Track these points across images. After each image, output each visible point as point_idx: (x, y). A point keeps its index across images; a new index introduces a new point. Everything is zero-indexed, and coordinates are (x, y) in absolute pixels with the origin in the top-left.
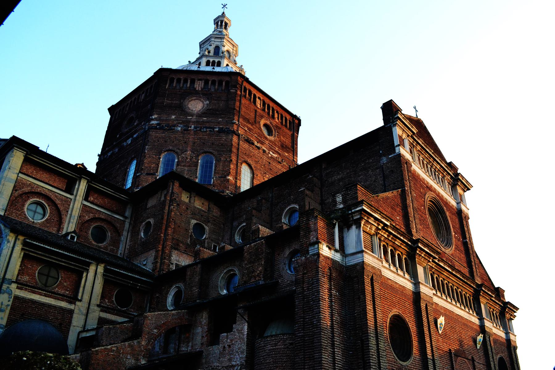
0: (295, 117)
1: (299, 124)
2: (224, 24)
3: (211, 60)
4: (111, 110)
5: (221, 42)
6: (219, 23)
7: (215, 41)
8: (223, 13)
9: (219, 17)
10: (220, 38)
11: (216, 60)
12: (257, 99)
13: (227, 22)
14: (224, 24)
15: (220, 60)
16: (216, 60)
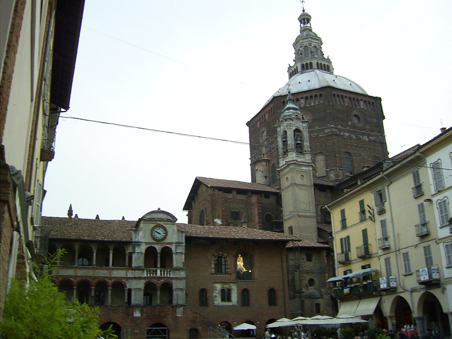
3: (304, 63)
4: (248, 124)
5: (308, 41)
7: (303, 42)
9: (301, 16)
11: (308, 62)
13: (309, 18)
14: (306, 21)
15: (311, 61)
16: (308, 62)
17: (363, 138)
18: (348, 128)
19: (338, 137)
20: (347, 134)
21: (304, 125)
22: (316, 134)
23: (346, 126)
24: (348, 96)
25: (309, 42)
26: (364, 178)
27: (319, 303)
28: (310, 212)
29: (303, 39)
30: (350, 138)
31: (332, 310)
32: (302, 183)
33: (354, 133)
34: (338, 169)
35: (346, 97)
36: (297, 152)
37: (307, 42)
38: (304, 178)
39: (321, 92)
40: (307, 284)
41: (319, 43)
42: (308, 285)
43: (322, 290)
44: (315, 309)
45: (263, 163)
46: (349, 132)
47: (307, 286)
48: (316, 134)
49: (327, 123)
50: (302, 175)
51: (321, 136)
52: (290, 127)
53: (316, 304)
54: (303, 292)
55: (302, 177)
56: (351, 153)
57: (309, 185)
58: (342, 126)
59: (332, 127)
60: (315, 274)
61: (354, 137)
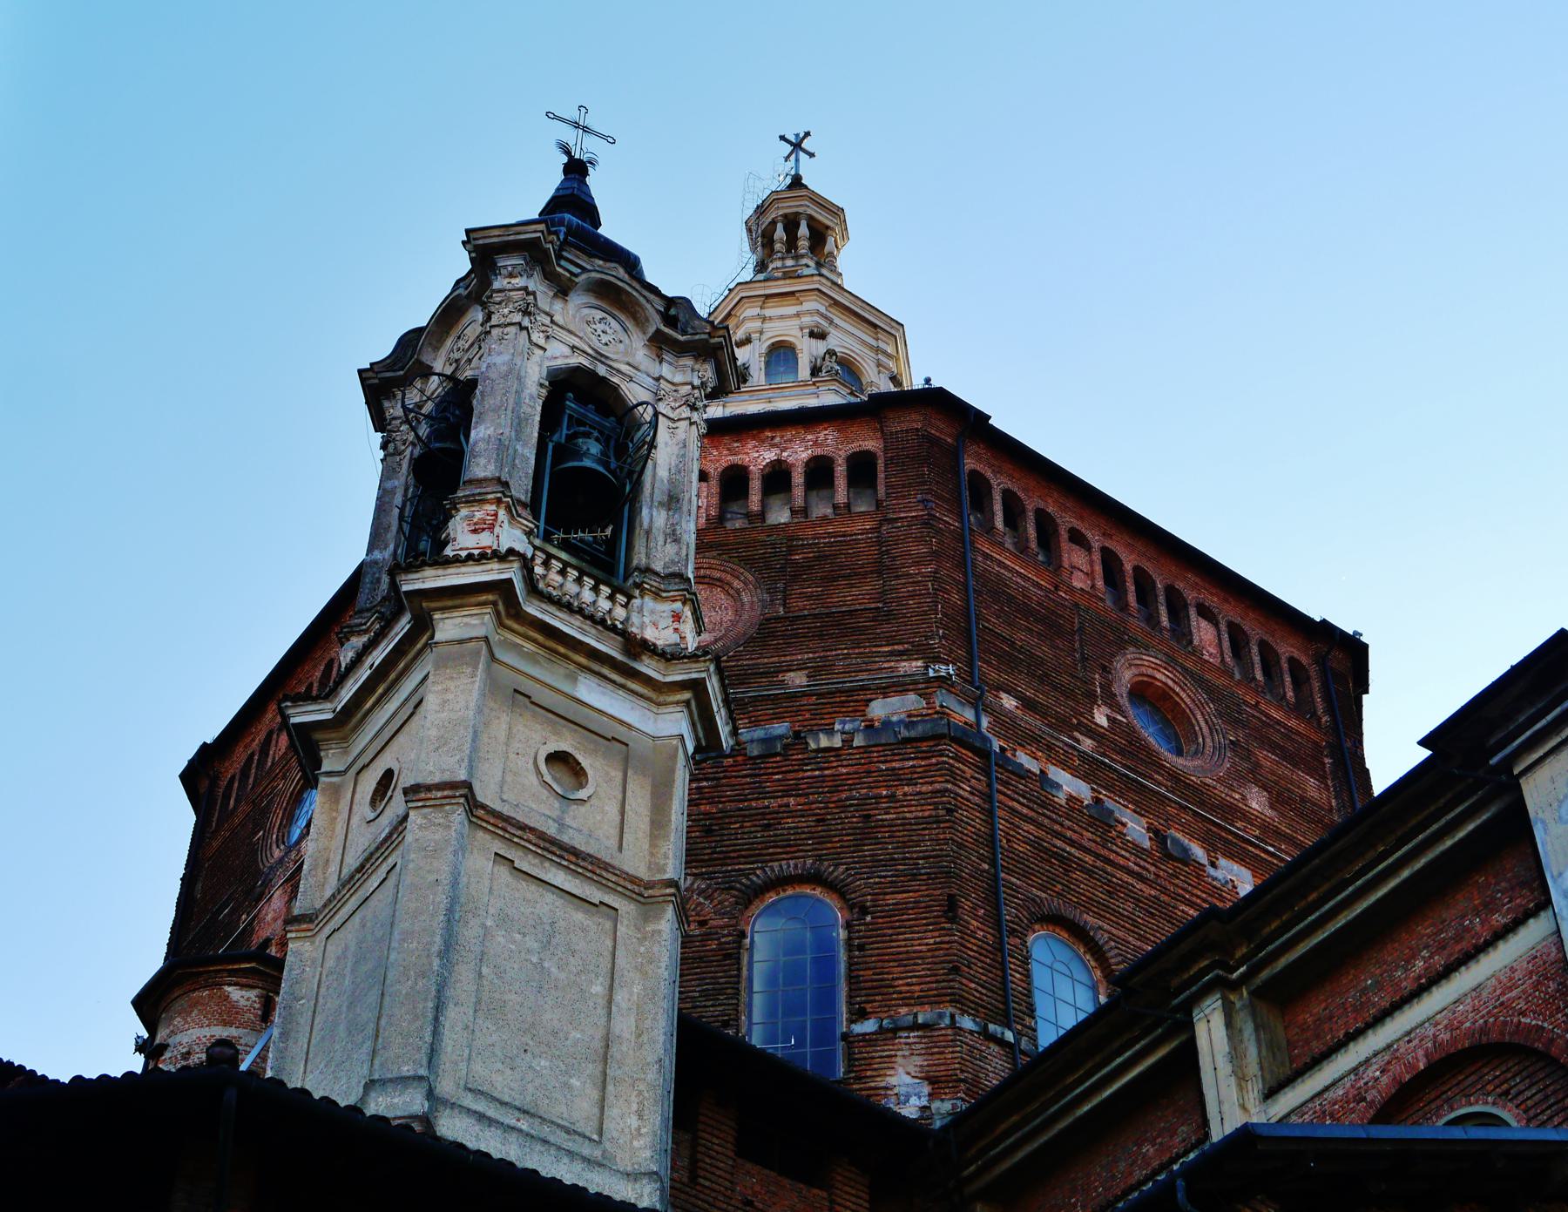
0: (1325, 632)
1: (1360, 681)
2: (803, 230)
5: (798, 315)
6: (780, 233)
7: (764, 319)
8: (797, 182)
9: (773, 199)
10: (792, 293)
12: (1065, 545)
13: (823, 217)
14: (803, 230)
17: (1211, 871)
18: (1087, 744)
19: (986, 772)
20: (1069, 785)
21: (666, 371)
22: (780, 728)
23: (1064, 725)
24: (1096, 540)
25: (807, 320)
26: (1265, 974)
28: (586, 1150)
29: (768, 296)
30: (1101, 821)
32: (551, 830)
33: (1144, 801)
34: (967, 1023)
35: (1077, 538)
36: (547, 538)
37: (796, 322)
38: (582, 794)
39: (871, 444)
41: (878, 350)
45: (235, 994)
46: (1088, 769)
48: (780, 728)
49: (901, 653)
50: (559, 759)
51: (824, 742)
52: (517, 318)
55: (561, 771)
56: (1102, 938)
57: (634, 880)
58: (1027, 704)
59: (942, 681)
61: (1136, 828)
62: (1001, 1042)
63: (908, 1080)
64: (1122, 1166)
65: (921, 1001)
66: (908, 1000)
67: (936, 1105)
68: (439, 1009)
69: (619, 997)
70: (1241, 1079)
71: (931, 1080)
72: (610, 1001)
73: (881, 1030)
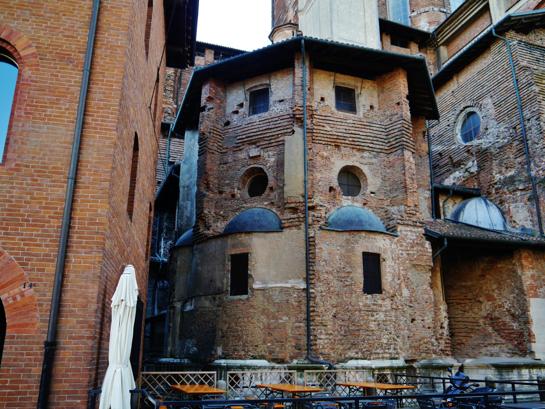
27: (375, 251)
31: (432, 285)
34: (436, 9)
40: (335, 183)
42: (339, 189)
43: (393, 209)
44: (359, 275)
47: (331, 189)
53: (364, 254)
54: (312, 208)
60: (366, 154)
62: (443, 12)
63: (424, 23)
64: (472, 33)
65: (426, 6)
66: (423, 7)
67: (430, 28)
68: (331, 23)
69: (366, 14)
70: (500, 9)
71: (430, 23)
72: (365, 16)
73: (418, 14)
